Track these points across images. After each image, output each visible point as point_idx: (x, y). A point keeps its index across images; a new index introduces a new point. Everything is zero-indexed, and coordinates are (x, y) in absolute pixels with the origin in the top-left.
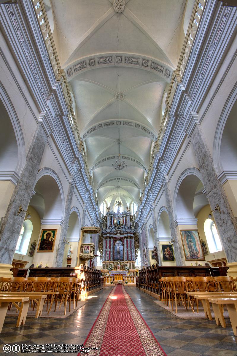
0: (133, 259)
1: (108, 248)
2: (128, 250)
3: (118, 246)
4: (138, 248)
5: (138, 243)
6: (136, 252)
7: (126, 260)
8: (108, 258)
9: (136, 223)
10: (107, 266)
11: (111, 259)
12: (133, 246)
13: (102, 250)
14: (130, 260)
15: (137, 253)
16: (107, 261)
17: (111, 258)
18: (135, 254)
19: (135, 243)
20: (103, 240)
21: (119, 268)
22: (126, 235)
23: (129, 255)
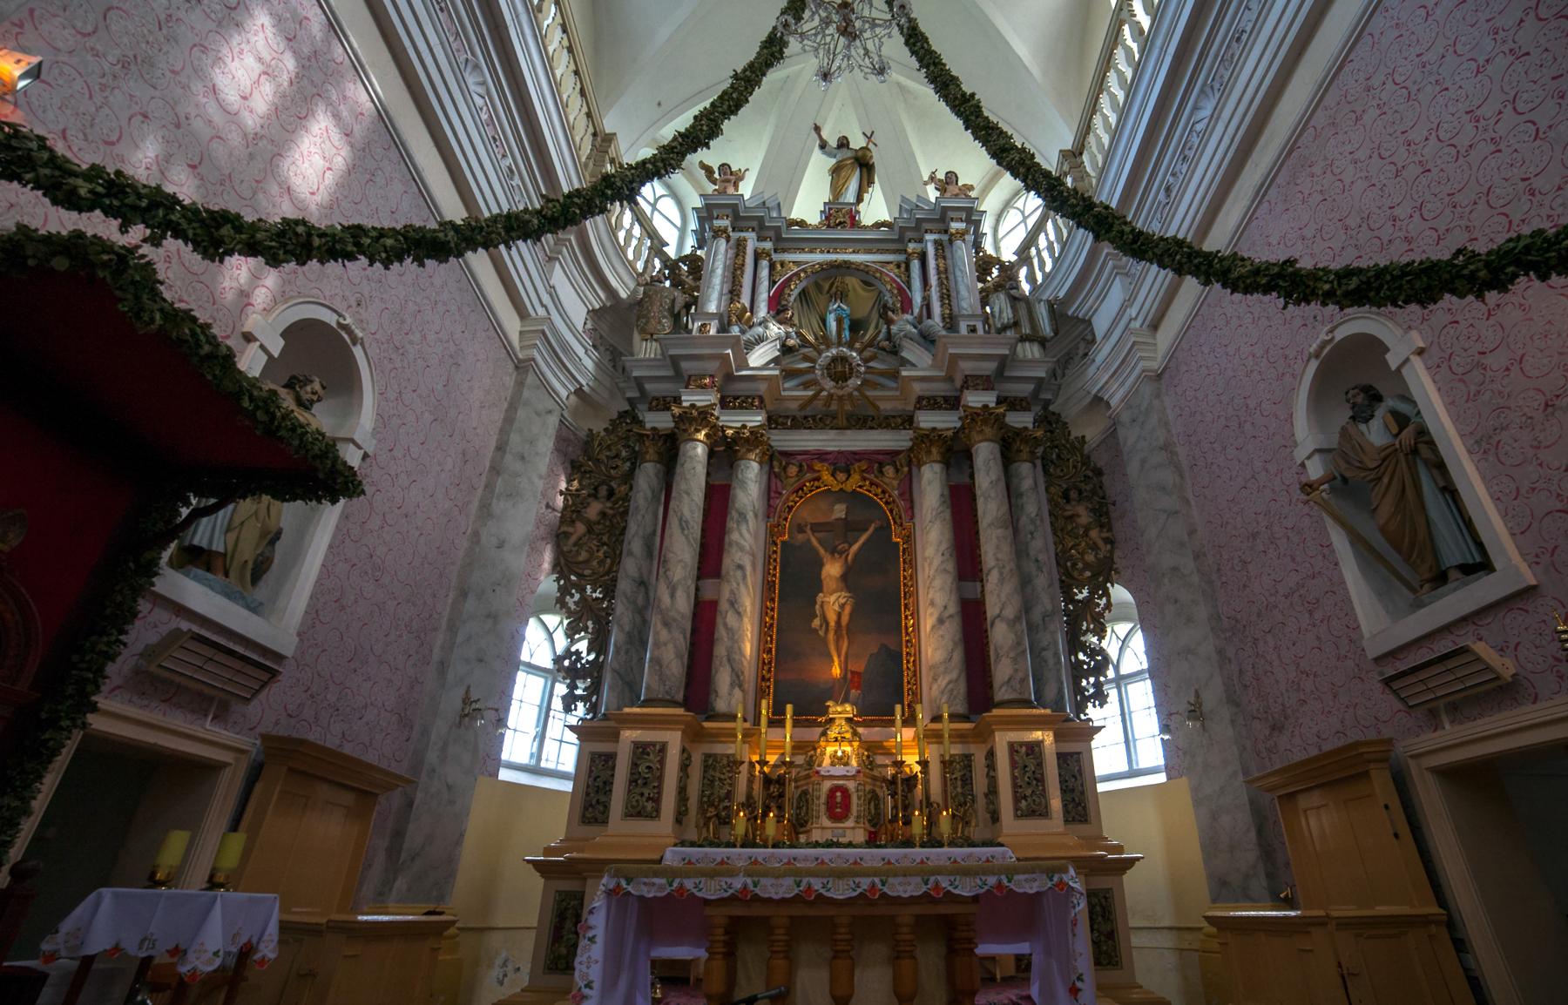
0: (1050, 693)
1: (683, 551)
2: (972, 589)
3: (833, 551)
4: (1102, 575)
5: (1103, 513)
6: (1086, 619)
7: (961, 708)
8: (676, 668)
9: (1057, 311)
10: (634, 780)
11: (727, 696)
12: (1041, 544)
13: (610, 592)
14: (1027, 703)
15: (1101, 632)
16: (649, 702)
17: (723, 679)
18: (1075, 644)
19: (1061, 525)
20: (629, 477)
21: (838, 805)
23: (1000, 635)
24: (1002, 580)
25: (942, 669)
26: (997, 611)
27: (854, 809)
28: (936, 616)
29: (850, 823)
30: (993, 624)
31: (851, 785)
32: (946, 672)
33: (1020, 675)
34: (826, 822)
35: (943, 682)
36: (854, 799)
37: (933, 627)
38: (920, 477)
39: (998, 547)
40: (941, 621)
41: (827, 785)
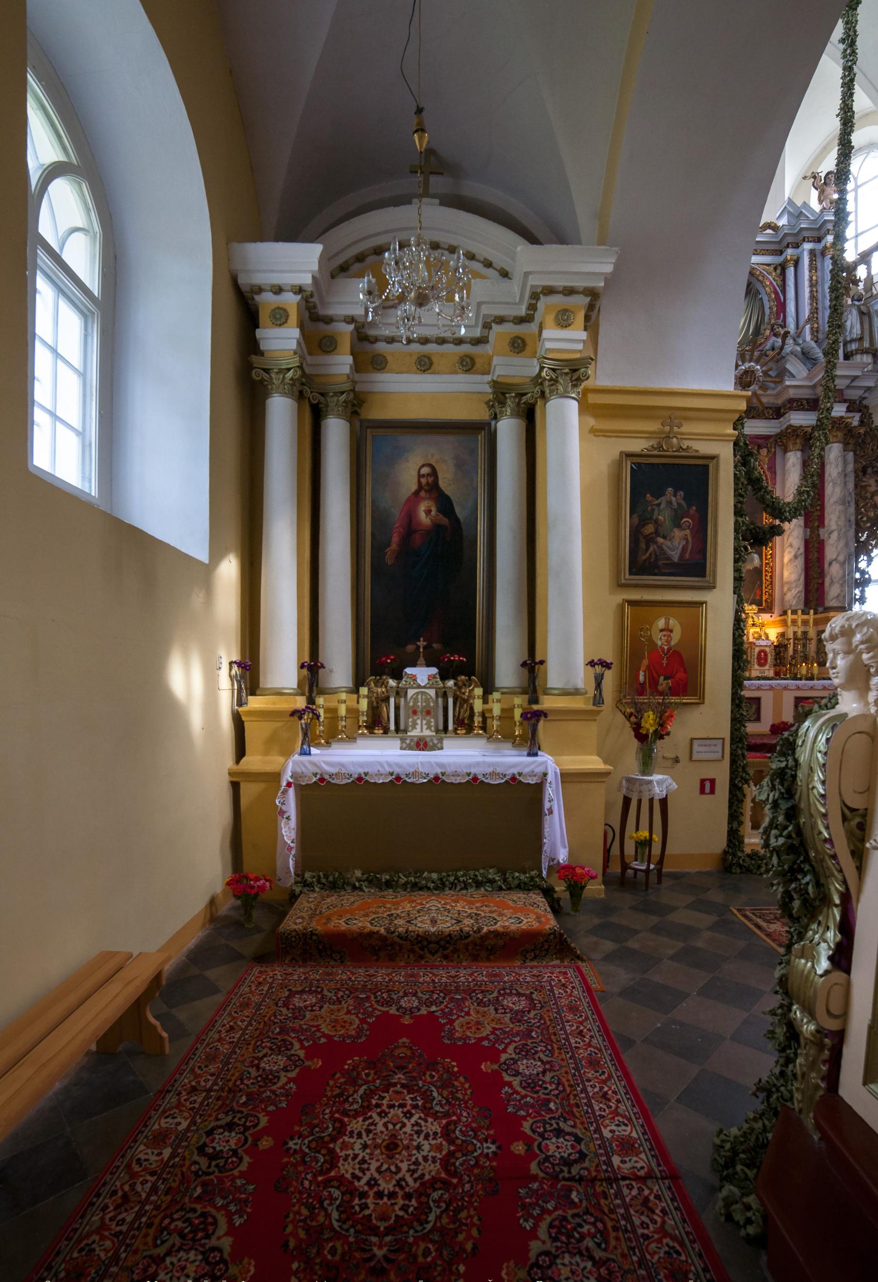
22: (801, 419)
24: (839, 538)
25: (794, 585)
26: (834, 557)
27: (769, 660)
28: (793, 554)
29: (767, 667)
30: (830, 564)
31: (767, 649)
32: (796, 587)
33: (843, 594)
34: (756, 667)
35: (794, 592)
36: (769, 657)
37: (790, 560)
38: (784, 461)
39: (839, 518)
40: (796, 557)
41: (757, 650)
